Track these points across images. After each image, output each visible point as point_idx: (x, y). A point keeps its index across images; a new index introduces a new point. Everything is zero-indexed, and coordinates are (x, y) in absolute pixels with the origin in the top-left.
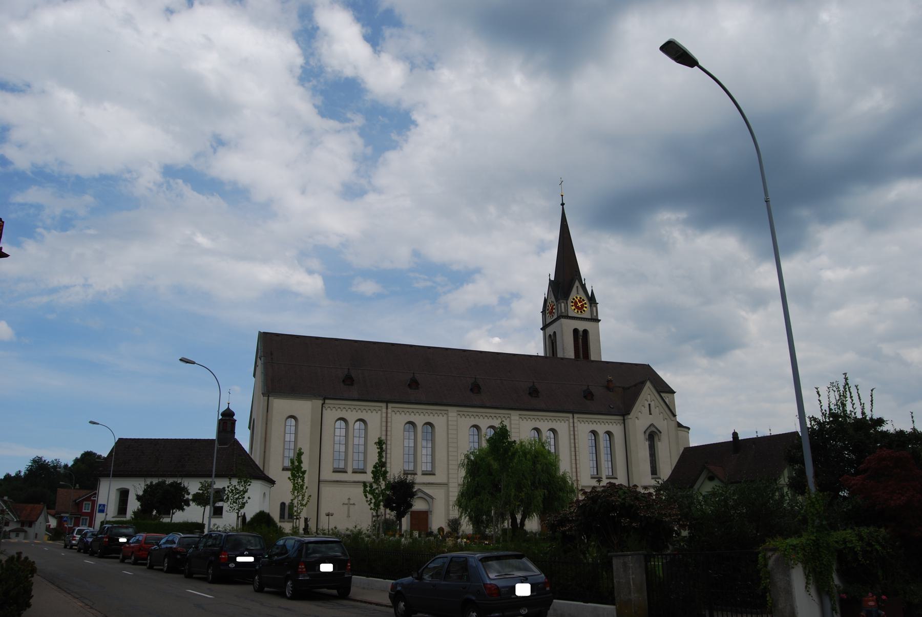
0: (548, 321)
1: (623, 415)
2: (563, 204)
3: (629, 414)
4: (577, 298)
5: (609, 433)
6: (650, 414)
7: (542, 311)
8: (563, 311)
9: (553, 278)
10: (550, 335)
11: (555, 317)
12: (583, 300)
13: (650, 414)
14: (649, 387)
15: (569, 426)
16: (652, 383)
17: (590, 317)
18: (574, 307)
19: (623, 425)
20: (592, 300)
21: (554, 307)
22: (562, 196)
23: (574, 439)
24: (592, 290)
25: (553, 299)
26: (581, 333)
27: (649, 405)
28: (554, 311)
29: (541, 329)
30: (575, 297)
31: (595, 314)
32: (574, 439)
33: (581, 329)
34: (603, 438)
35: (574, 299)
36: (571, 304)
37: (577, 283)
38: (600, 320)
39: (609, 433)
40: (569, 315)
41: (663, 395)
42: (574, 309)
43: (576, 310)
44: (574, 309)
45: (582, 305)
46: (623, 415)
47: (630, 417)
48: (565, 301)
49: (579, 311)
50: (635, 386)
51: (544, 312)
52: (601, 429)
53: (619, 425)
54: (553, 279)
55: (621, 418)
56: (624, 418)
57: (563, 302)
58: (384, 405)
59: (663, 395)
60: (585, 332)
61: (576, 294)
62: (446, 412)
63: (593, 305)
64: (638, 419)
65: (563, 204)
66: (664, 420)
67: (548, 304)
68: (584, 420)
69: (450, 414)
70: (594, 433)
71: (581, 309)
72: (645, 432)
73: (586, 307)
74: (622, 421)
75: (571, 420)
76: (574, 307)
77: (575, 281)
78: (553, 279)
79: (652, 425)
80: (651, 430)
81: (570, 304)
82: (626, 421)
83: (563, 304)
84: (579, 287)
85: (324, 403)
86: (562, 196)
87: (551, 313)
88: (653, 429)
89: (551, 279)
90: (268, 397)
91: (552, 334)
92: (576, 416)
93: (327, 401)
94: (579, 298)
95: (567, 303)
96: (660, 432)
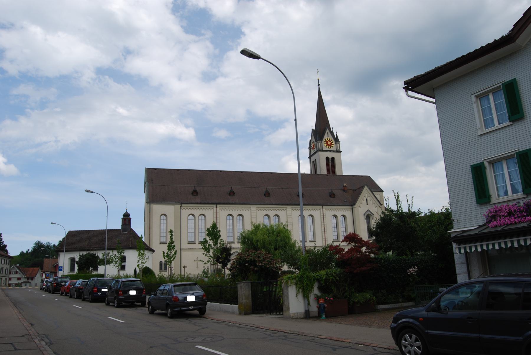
0: (312, 153)
1: (352, 206)
2: (319, 85)
3: (355, 205)
4: (327, 139)
5: (344, 216)
6: (367, 204)
7: (308, 147)
8: (320, 147)
9: (314, 128)
10: (313, 161)
11: (316, 150)
12: (332, 140)
13: (367, 204)
14: (366, 189)
15: (321, 213)
16: (368, 186)
17: (336, 150)
18: (326, 145)
19: (352, 211)
20: (336, 139)
21: (315, 145)
22: (318, 80)
23: (324, 220)
24: (337, 134)
25: (314, 140)
26: (330, 159)
27: (367, 199)
28: (315, 147)
29: (309, 158)
31: (338, 148)
32: (324, 220)
33: (330, 157)
34: (340, 218)
35: (326, 140)
36: (325, 143)
37: (327, 131)
38: (341, 151)
39: (344, 216)
40: (323, 149)
41: (374, 193)
42: (326, 146)
44: (326, 146)
45: (331, 143)
46: (352, 206)
47: (355, 206)
48: (321, 142)
49: (329, 147)
50: (359, 189)
51: (309, 148)
52: (339, 214)
53: (349, 211)
54: (314, 129)
55: (351, 207)
56: (352, 207)
57: (320, 142)
58: (215, 206)
59: (374, 193)
60: (333, 159)
61: (327, 137)
62: (250, 208)
63: (337, 143)
64: (360, 208)
65: (319, 85)
66: (375, 208)
67: (312, 143)
68: (329, 209)
69: (252, 209)
70: (335, 216)
71: (330, 145)
72: (364, 215)
73: (333, 144)
74: (351, 209)
75: (322, 210)
76: (326, 145)
77: (326, 130)
78: (314, 129)
79: (368, 210)
80: (367, 213)
81: (324, 143)
82: (353, 209)
83: (319, 144)
85: (181, 206)
86: (318, 80)
87: (313, 148)
88: (369, 213)
89: (313, 129)
90: (150, 204)
91: (314, 160)
92: (324, 207)
93: (183, 205)
94: (329, 139)
95: (322, 143)
96: (373, 214)
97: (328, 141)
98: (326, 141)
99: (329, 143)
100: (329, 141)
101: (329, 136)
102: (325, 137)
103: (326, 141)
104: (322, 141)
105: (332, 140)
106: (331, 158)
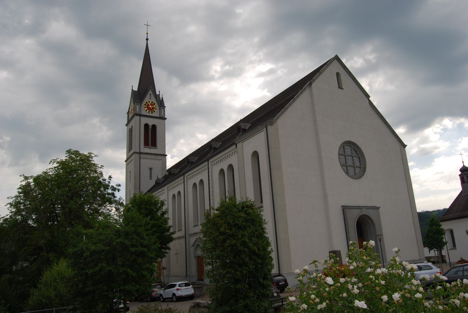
2: (147, 39)
4: (149, 102)
9: (136, 89)
12: (154, 104)
17: (159, 116)
18: (146, 109)
20: (161, 104)
24: (162, 97)
26: (150, 127)
30: (148, 102)
31: (163, 114)
35: (147, 103)
36: (144, 106)
37: (150, 92)
38: (166, 119)
40: (142, 114)
42: (147, 110)
43: (148, 111)
44: (147, 110)
45: (153, 108)
48: (140, 104)
54: (137, 90)
57: (138, 105)
60: (154, 127)
61: (149, 99)
63: (161, 108)
65: (147, 39)
71: (152, 110)
73: (156, 109)
76: (146, 109)
78: (137, 90)
81: (143, 105)
84: (152, 96)
86: (147, 34)
89: (134, 89)
94: (151, 102)
95: (141, 105)
97: (150, 104)
98: (147, 104)
99: (151, 106)
100: (152, 105)
102: (147, 99)
103: (147, 104)
104: (141, 103)
105: (154, 104)
106: (151, 125)
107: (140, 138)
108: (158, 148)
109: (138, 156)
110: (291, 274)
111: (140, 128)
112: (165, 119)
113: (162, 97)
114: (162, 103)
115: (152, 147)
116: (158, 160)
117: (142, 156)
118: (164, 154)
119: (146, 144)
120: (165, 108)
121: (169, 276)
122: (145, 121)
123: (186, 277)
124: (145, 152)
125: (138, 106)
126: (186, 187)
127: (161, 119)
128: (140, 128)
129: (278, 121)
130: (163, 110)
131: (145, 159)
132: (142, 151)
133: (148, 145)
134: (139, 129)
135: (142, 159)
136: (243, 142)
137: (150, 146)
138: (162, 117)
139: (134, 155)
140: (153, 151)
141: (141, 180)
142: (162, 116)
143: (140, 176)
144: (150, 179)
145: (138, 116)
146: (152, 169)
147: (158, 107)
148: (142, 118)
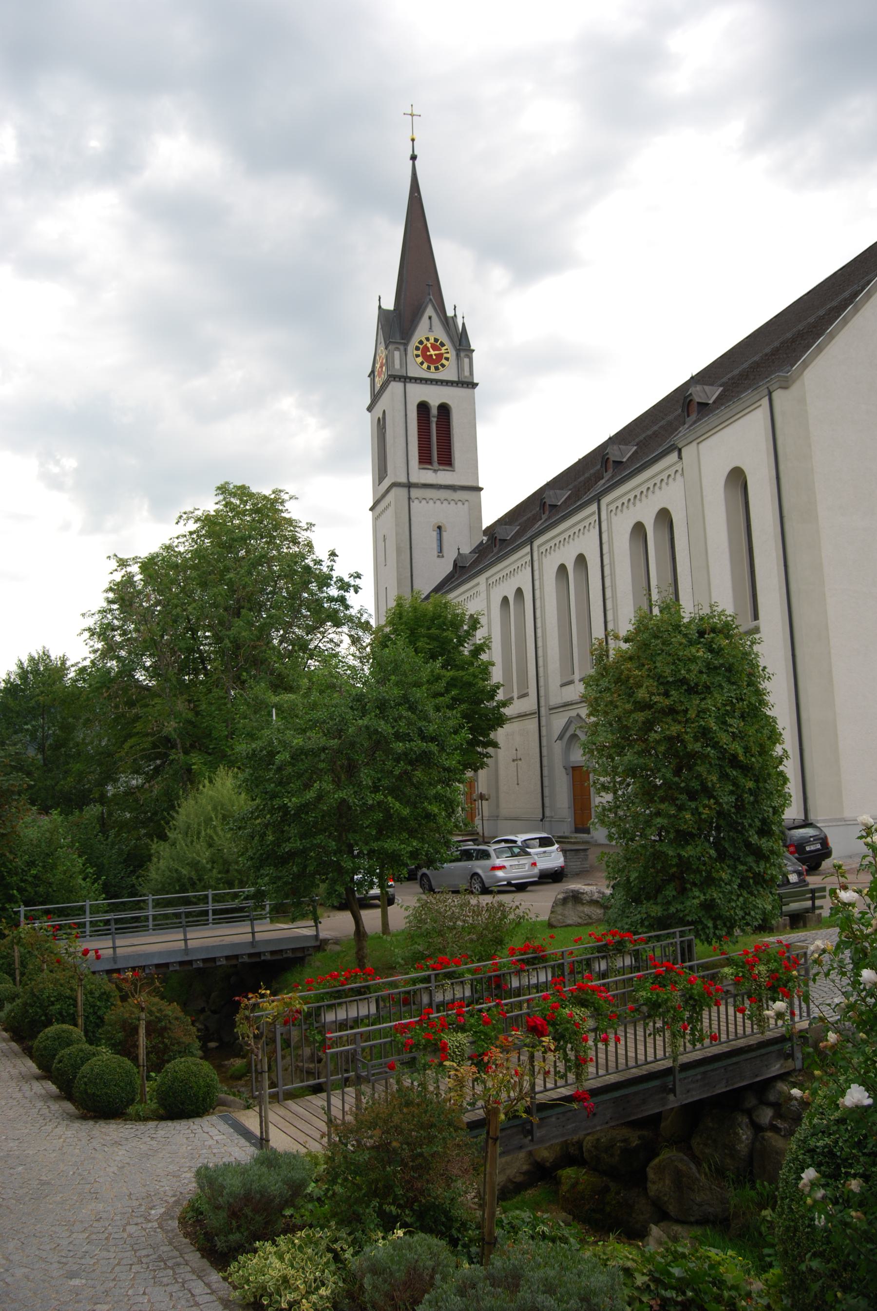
2: (414, 158)
4: (428, 339)
9: (389, 304)
12: (442, 345)
17: (456, 379)
18: (420, 359)
22: (413, 140)
24: (464, 324)
26: (434, 411)
31: (467, 373)
35: (421, 342)
36: (416, 352)
37: (430, 311)
38: (477, 384)
40: (410, 374)
42: (422, 363)
43: (425, 365)
44: (422, 363)
45: (440, 357)
48: (402, 348)
57: (397, 349)
60: (444, 410)
63: (462, 354)
65: (414, 158)
71: (435, 362)
73: (447, 359)
76: (420, 359)
84: (436, 320)
86: (413, 140)
89: (384, 306)
94: (432, 341)
95: (406, 350)
97: (429, 345)
98: (421, 347)
99: (432, 352)
100: (435, 348)
101: (433, 328)
102: (421, 333)
104: (406, 345)
105: (442, 345)
106: (437, 404)
107: (407, 444)
108: (456, 469)
109: (403, 492)
110: (839, 823)
111: (406, 415)
112: (474, 385)
113: (464, 324)
114: (464, 340)
115: (441, 468)
116: (460, 503)
117: (415, 493)
118: (474, 484)
119: (425, 459)
120: (474, 354)
121: (497, 817)
122: (418, 393)
123: (542, 820)
124: (423, 481)
125: (397, 354)
126: (537, 576)
127: (462, 387)
128: (406, 415)
129: (805, 373)
130: (466, 360)
131: (424, 502)
132: (414, 479)
133: (430, 463)
134: (403, 420)
135: (416, 501)
136: (698, 443)
137: (436, 465)
138: (464, 380)
139: (394, 490)
140: (443, 477)
141: (414, 561)
142: (466, 377)
143: (411, 548)
144: (438, 556)
145: (400, 381)
146: (443, 529)
147: (454, 353)
148: (411, 387)
